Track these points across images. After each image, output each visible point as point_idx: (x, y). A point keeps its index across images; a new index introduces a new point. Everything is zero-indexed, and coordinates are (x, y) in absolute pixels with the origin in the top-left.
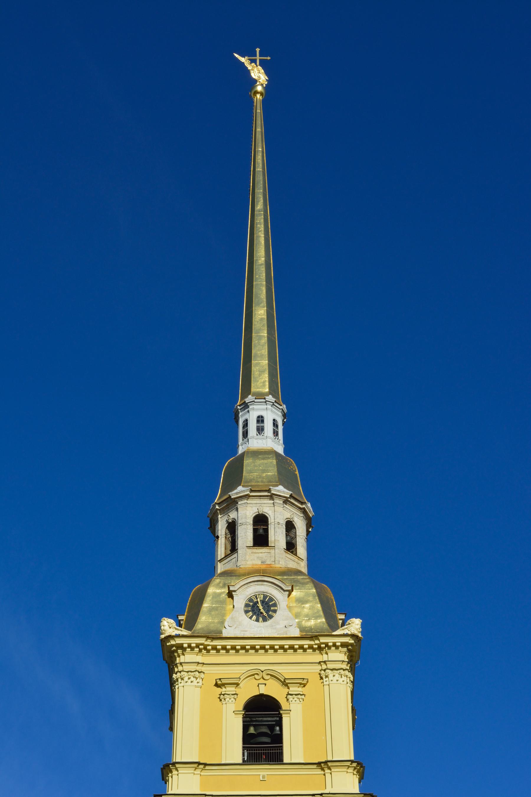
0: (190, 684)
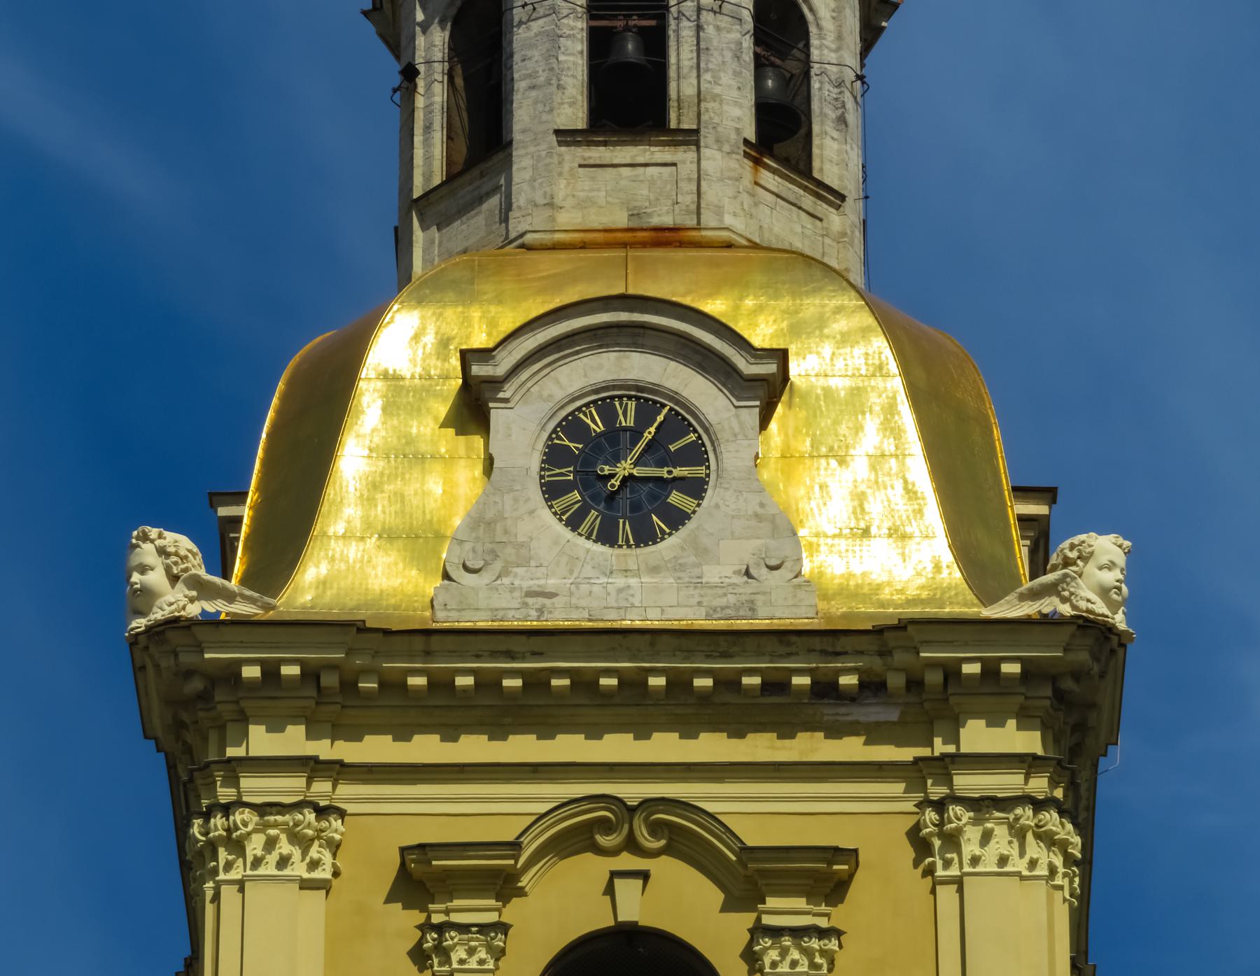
0: (276, 872)
